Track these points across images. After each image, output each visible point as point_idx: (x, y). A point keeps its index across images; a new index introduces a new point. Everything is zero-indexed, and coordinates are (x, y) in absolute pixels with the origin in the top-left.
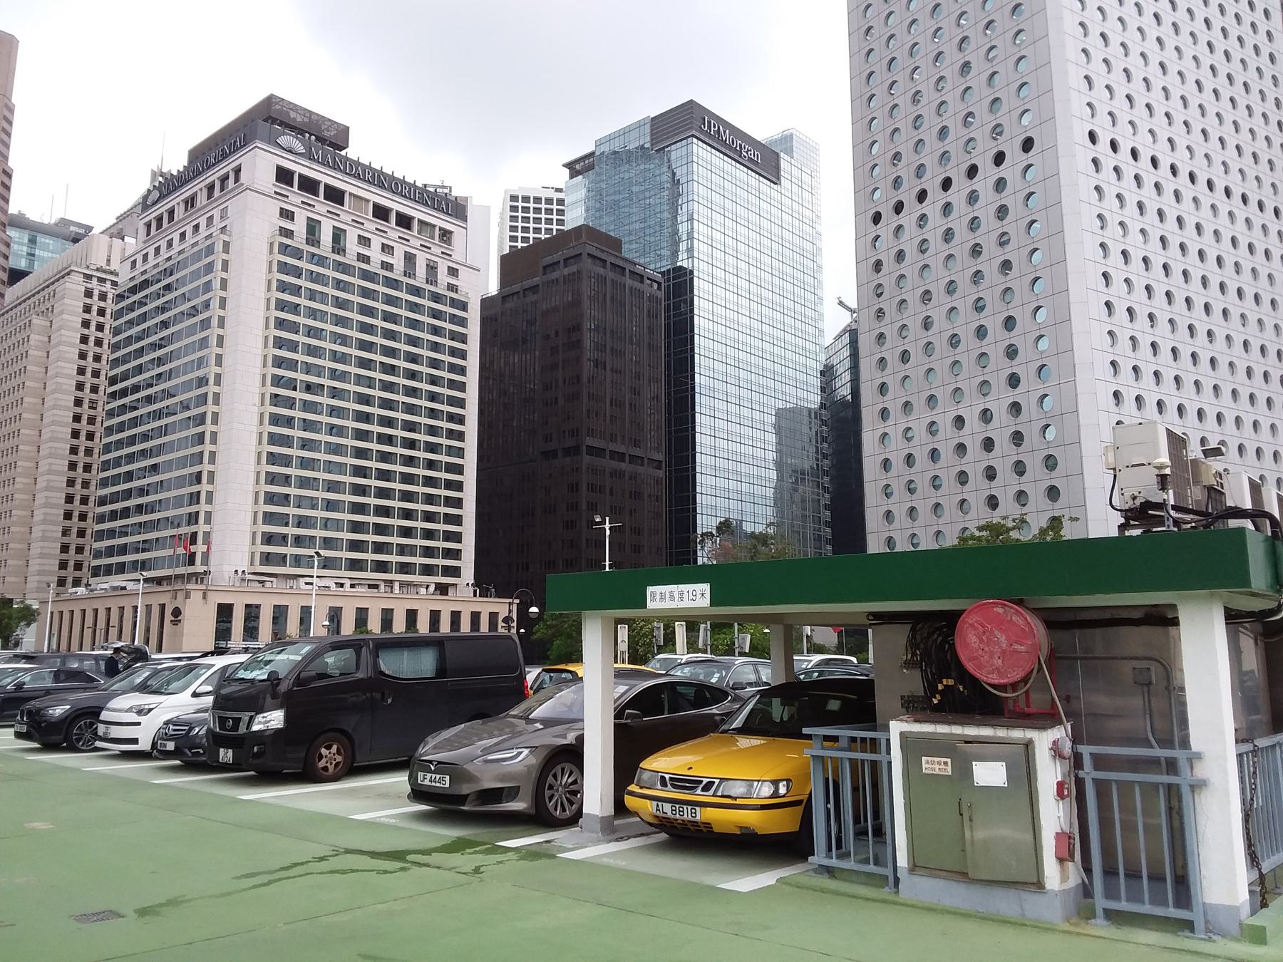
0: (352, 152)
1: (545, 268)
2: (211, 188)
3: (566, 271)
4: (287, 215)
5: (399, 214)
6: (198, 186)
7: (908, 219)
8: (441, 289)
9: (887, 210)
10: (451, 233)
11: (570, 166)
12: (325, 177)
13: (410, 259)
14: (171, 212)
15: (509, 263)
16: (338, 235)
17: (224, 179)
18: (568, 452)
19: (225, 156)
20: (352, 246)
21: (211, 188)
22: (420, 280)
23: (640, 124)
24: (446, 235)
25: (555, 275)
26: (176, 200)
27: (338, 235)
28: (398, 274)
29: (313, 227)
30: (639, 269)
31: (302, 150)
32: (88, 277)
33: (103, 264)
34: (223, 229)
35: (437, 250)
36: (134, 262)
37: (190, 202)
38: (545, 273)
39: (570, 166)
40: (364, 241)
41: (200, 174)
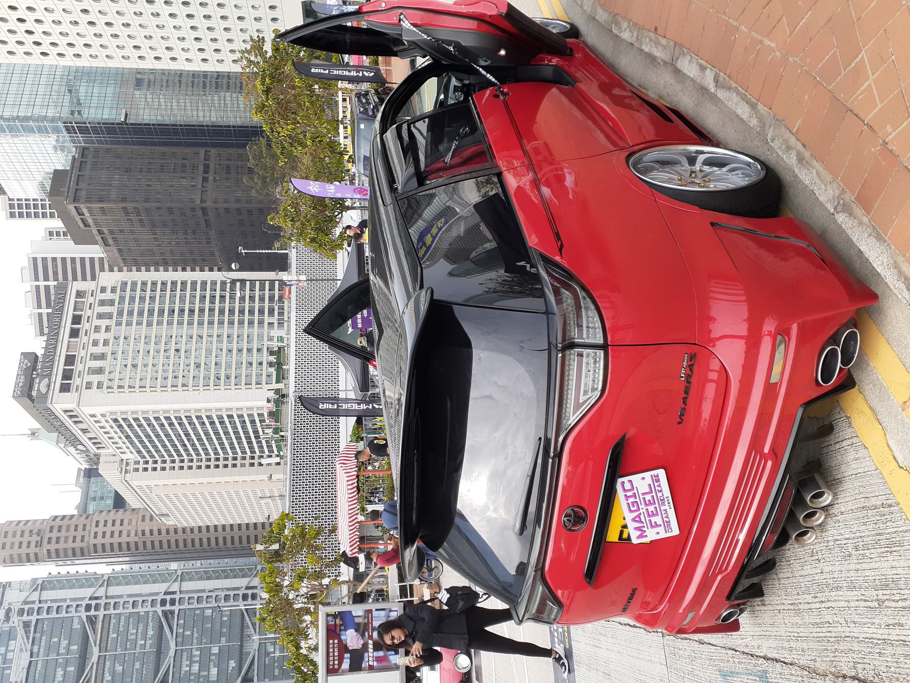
0: (40, 352)
1: (86, 226)
2: (76, 422)
3: (87, 214)
4: (89, 386)
5: (73, 323)
6: (76, 429)
8: (116, 297)
10: (77, 291)
12: (60, 367)
13: (100, 316)
14: (90, 439)
15: (80, 239)
17: (71, 417)
19: (56, 417)
20: (100, 349)
21: (76, 422)
22: (113, 310)
24: (80, 294)
25: (90, 221)
26: (84, 438)
30: (77, 165)
31: (46, 381)
32: (126, 472)
33: (117, 465)
37: (84, 431)
38: (89, 226)
40: (95, 343)
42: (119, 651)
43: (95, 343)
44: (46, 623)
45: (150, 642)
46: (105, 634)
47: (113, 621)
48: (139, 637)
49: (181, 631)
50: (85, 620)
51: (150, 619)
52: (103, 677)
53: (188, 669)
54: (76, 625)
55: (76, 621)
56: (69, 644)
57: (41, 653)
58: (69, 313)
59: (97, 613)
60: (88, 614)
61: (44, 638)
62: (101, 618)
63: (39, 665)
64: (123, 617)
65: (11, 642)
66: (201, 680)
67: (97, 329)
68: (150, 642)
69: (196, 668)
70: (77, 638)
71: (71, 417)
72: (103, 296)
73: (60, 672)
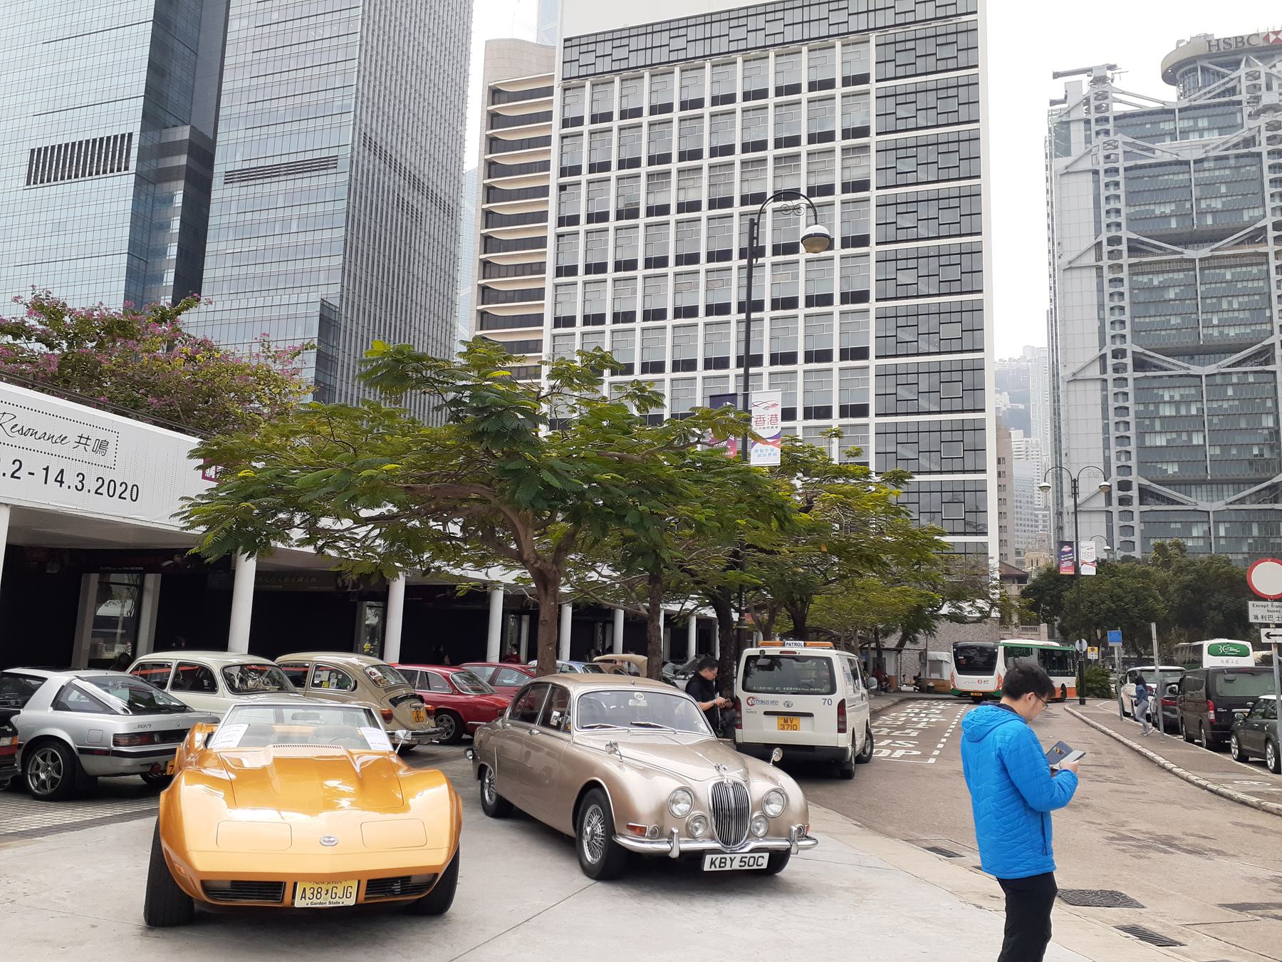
42: (1200, 289)
44: (1254, 168)
45: (1216, 334)
46: (1233, 261)
47: (1255, 270)
48: (1225, 315)
49: (1235, 379)
50: (1259, 225)
51: (1258, 327)
52: (1158, 273)
53: (1167, 398)
54: (1246, 216)
55: (1257, 213)
56: (1214, 212)
57: (1201, 175)
59: (1271, 241)
60: (1270, 228)
61: (1227, 172)
62: (1261, 249)
63: (1181, 177)
64: (1261, 283)
65: (1216, 132)
66: (1147, 422)
68: (1216, 334)
69: (1167, 411)
70: (1226, 221)
73: (1167, 209)
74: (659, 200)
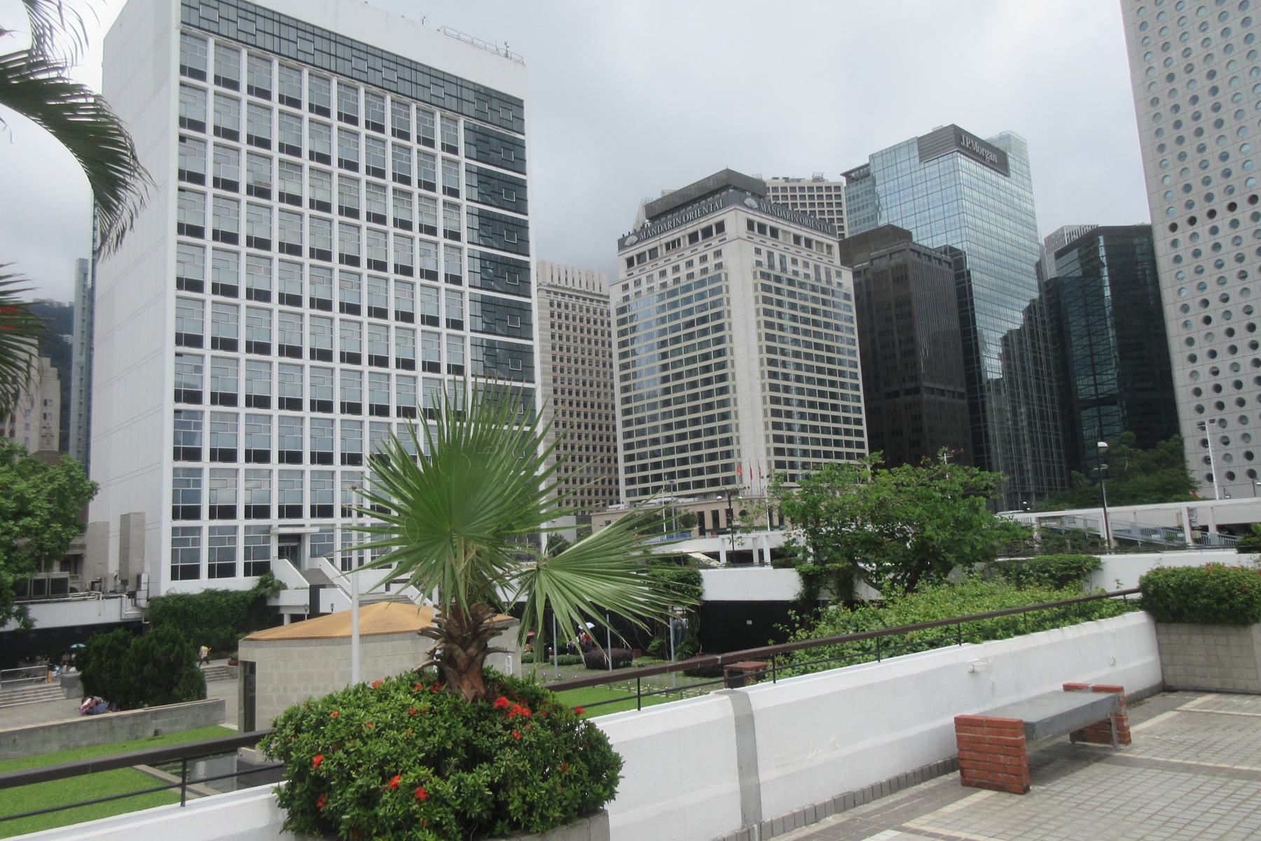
3: (893, 262)
4: (758, 251)
6: (681, 233)
7: (1203, 227)
9: (1182, 222)
11: (846, 175)
12: (770, 222)
13: (817, 268)
16: (782, 258)
18: (908, 392)
19: (703, 214)
20: (790, 267)
23: (908, 143)
24: (829, 247)
27: (782, 258)
28: (812, 281)
29: (770, 255)
32: (548, 292)
33: (549, 281)
34: (719, 266)
35: (826, 260)
36: (626, 287)
39: (846, 175)
40: (794, 261)
41: (678, 225)
43: (794, 261)
58: (815, 236)
67: (806, 265)
71: (707, 232)
72: (833, 274)
74: (292, 189)
